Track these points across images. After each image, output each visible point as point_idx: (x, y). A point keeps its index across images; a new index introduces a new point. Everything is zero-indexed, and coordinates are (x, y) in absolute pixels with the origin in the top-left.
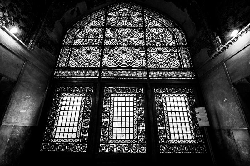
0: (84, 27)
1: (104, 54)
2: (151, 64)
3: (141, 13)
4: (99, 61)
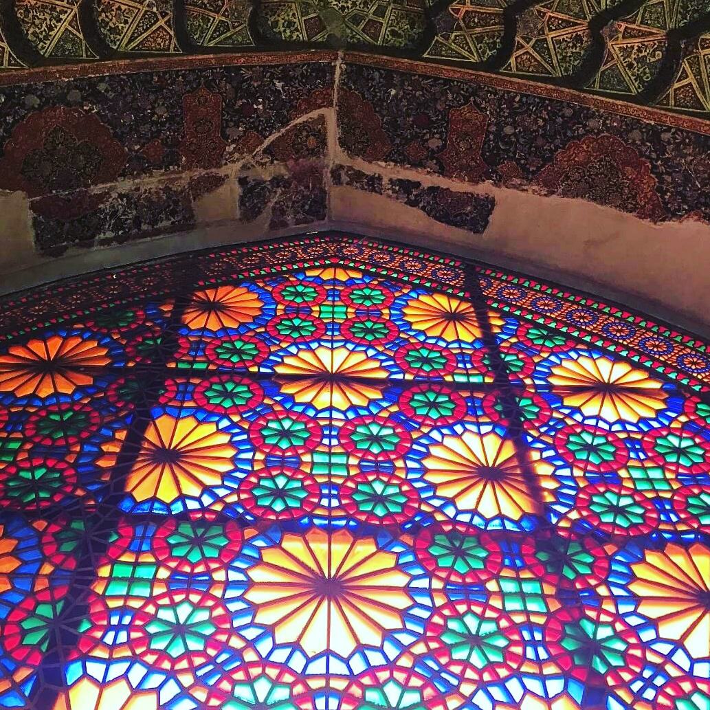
1: (103, 598)
3: (462, 300)
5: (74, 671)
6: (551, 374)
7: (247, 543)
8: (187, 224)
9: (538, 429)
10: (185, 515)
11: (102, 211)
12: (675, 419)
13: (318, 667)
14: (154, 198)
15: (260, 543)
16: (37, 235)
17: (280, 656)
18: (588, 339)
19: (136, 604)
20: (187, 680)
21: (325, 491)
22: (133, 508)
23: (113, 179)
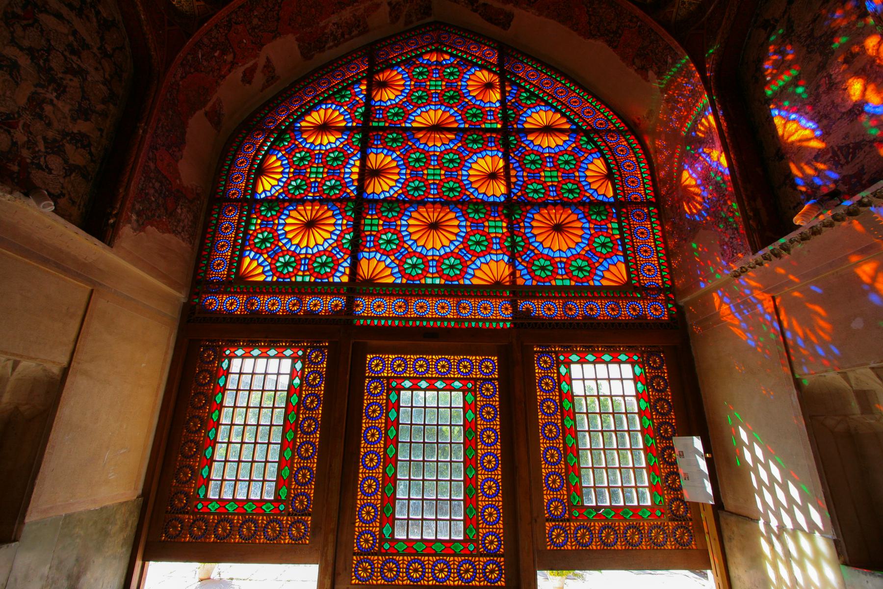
0: (291, 128)
4: (345, 260)
10: (385, 199)
16: (301, 52)
17: (419, 250)
19: (374, 233)
20: (393, 258)
21: (432, 187)
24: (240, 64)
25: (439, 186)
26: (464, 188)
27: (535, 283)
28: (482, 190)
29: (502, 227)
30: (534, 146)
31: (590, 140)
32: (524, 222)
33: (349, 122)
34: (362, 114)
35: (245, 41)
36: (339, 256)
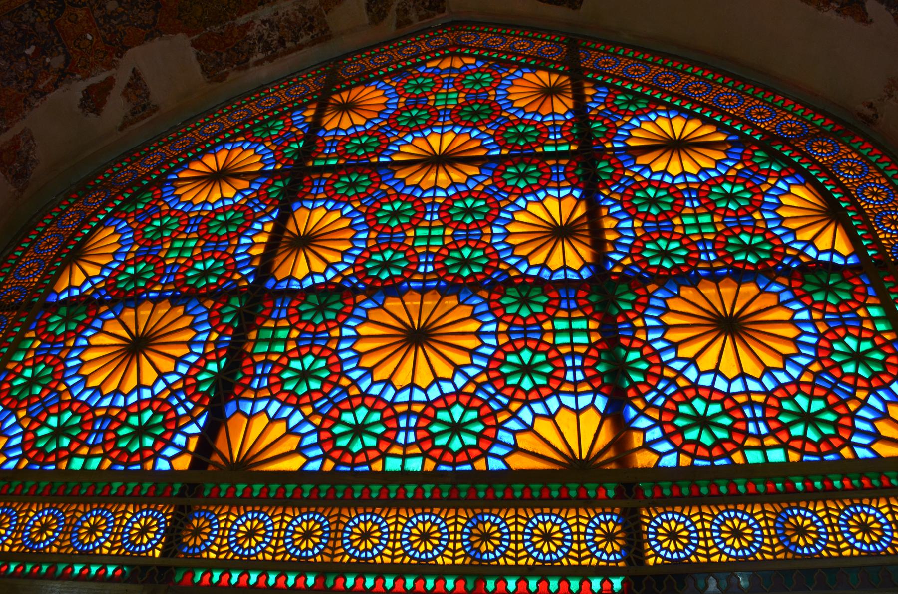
2: (656, 433)
3: (561, 74)
4: (194, 420)
5: (231, 407)
6: (630, 136)
7: (356, 306)
8: (325, 36)
9: (609, 188)
10: (314, 288)
11: (250, 38)
12: (732, 168)
13: (404, 396)
14: (293, 19)
15: (369, 305)
16: (202, 67)
17: (376, 390)
18: (668, 100)
19: (275, 358)
20: (308, 410)
22: (275, 285)
23: (254, 8)
24: (78, 76)
25: (438, 258)
26: (495, 257)
27: (685, 461)
28: (539, 259)
29: (588, 332)
30: (653, 174)
31: (774, 156)
32: (643, 317)
33: (270, 165)
34: (297, 151)
35: (89, 37)
36: (181, 411)
